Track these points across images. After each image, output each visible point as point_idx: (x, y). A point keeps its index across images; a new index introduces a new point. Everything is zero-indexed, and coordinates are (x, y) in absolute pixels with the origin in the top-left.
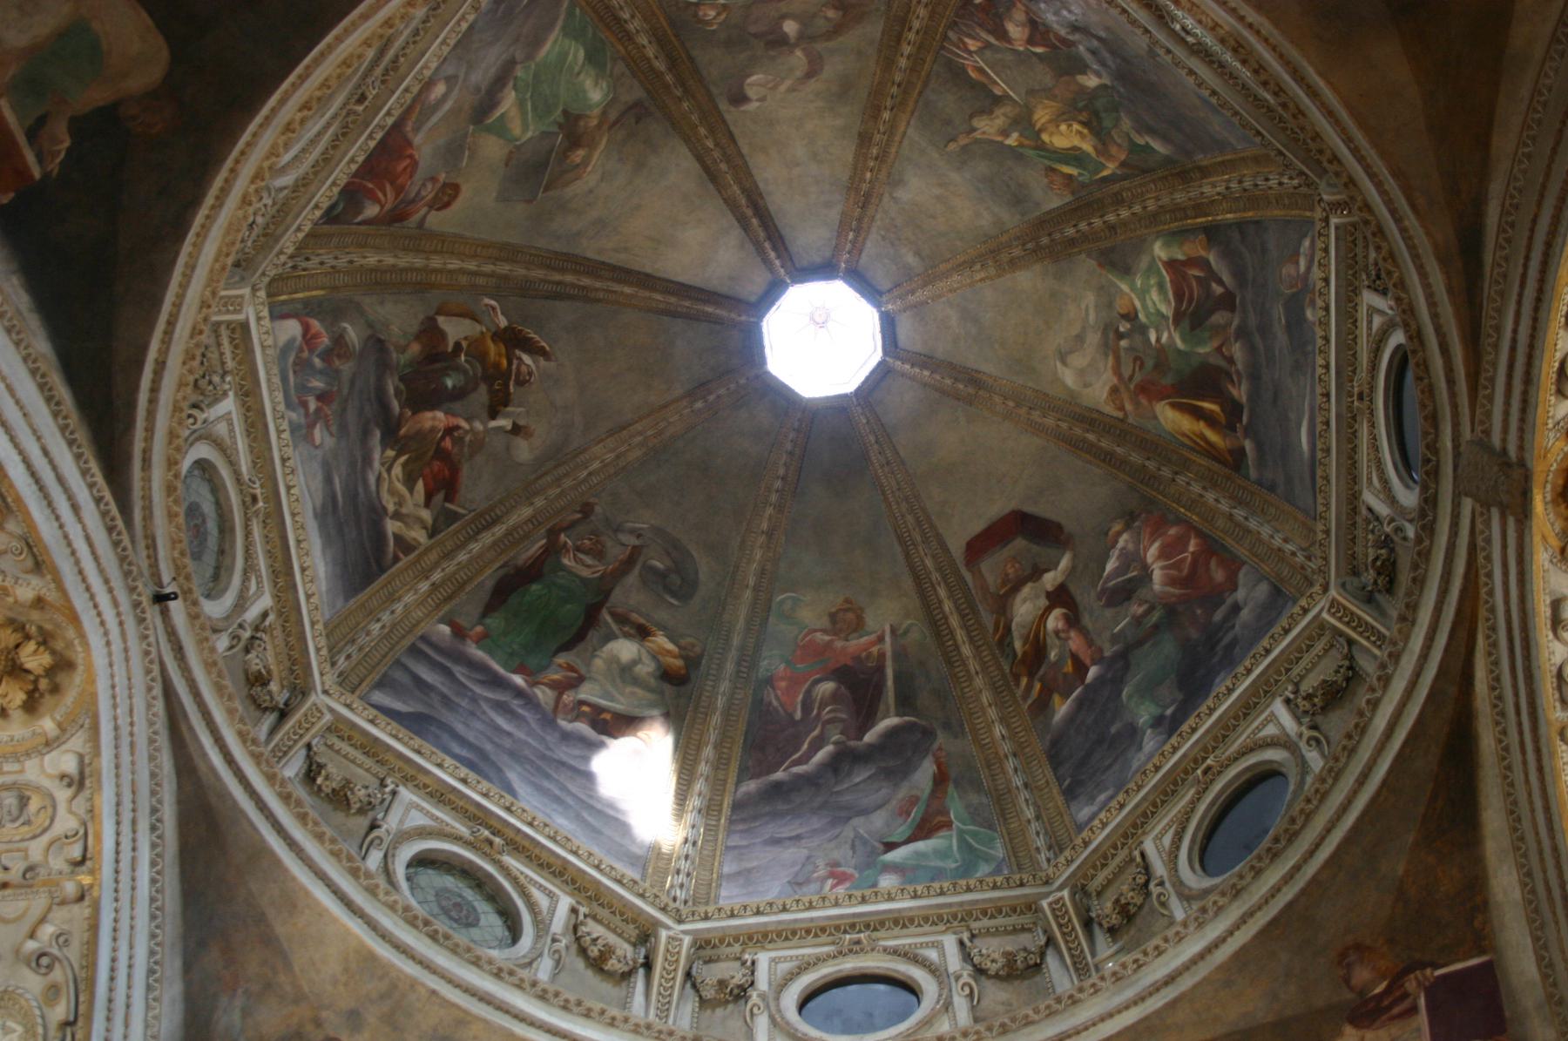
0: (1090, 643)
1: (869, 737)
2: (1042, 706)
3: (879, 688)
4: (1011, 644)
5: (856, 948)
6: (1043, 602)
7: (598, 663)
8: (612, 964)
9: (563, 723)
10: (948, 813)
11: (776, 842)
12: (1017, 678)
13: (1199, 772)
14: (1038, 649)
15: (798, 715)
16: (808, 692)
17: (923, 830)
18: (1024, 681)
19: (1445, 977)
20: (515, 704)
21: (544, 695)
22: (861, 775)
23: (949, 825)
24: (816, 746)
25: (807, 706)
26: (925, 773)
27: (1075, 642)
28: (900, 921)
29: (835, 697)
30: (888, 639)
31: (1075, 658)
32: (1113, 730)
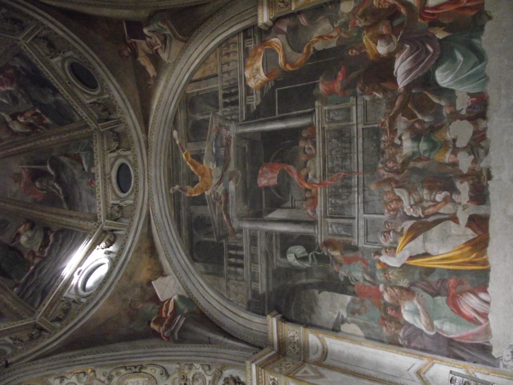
0: (29, 110)
1: (52, 173)
2: (47, 126)
3: (38, 170)
4: (28, 133)
5: (110, 179)
6: (15, 122)
7: (27, 246)
8: (112, 239)
9: (45, 255)
10: (76, 154)
11: (81, 199)
12: (37, 132)
13: (69, 85)
14: (29, 125)
15: (45, 192)
16: (39, 189)
17: (80, 161)
18: (39, 130)
19: (128, 34)
20: (39, 269)
21: (37, 261)
22: (63, 176)
23: (78, 154)
24: (54, 187)
25: (43, 190)
26: (64, 159)
27: (28, 114)
28: (104, 167)
29: (41, 182)
30: (24, 167)
31: (33, 115)
32: (55, 107)
